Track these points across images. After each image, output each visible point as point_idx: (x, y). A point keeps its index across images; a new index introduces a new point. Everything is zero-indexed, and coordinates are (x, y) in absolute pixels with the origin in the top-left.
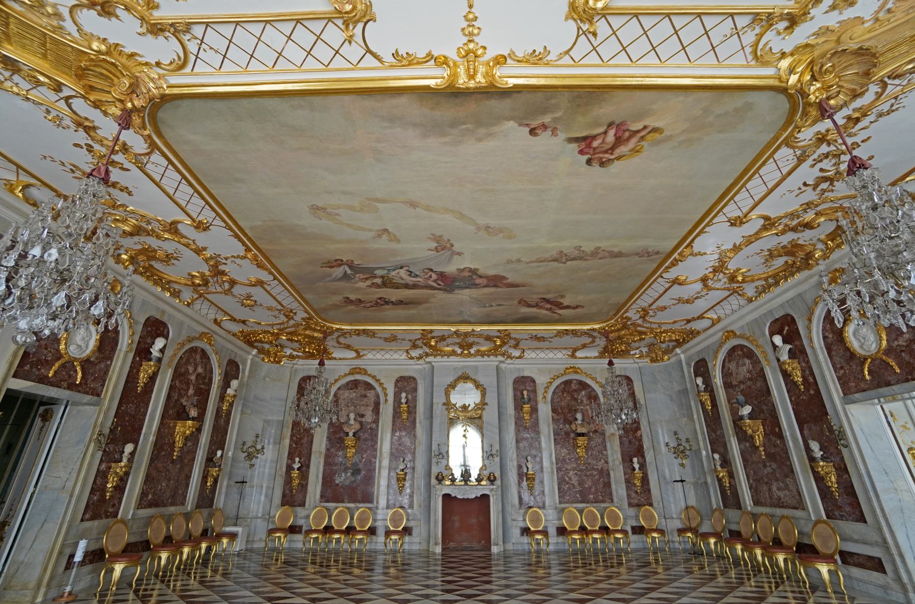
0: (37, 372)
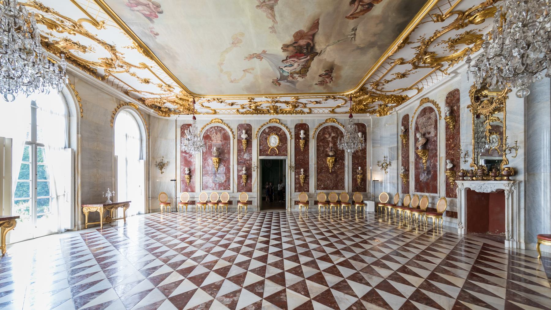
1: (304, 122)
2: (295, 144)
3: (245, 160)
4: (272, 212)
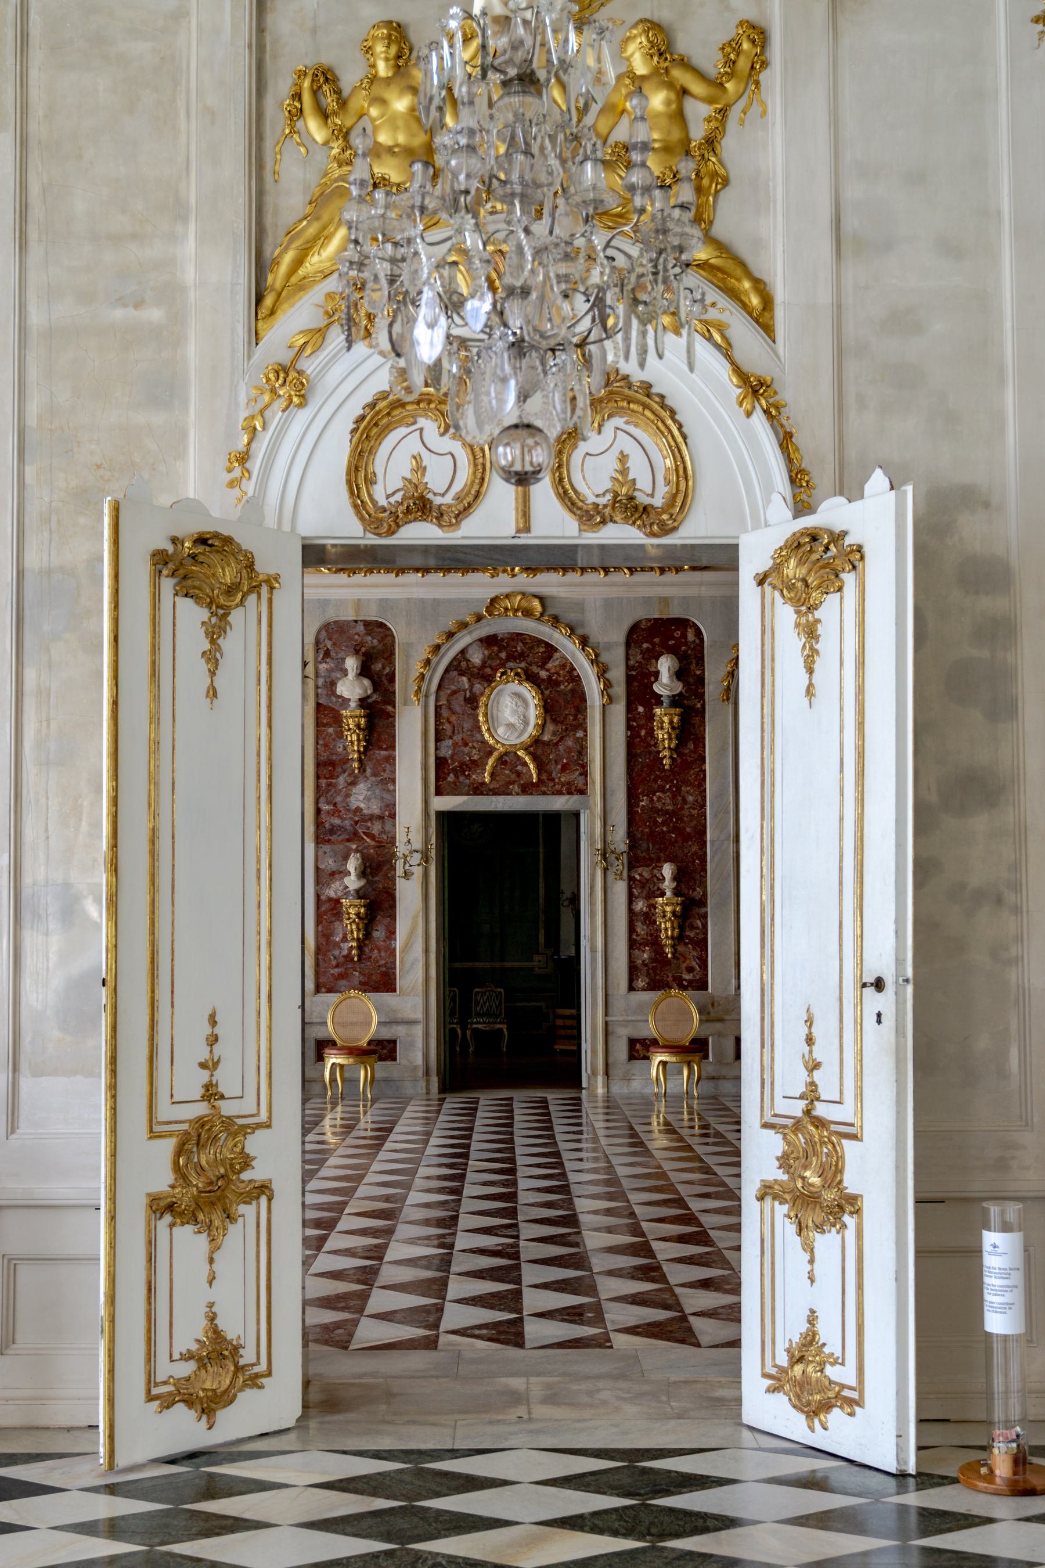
0: (467, 781)
1: (675, 612)
2: (629, 727)
3: (361, 817)
4: (511, 1099)
